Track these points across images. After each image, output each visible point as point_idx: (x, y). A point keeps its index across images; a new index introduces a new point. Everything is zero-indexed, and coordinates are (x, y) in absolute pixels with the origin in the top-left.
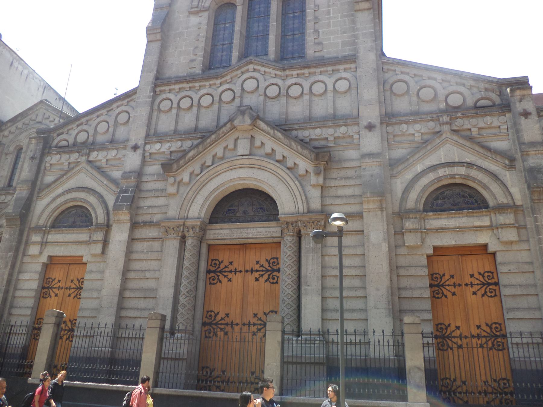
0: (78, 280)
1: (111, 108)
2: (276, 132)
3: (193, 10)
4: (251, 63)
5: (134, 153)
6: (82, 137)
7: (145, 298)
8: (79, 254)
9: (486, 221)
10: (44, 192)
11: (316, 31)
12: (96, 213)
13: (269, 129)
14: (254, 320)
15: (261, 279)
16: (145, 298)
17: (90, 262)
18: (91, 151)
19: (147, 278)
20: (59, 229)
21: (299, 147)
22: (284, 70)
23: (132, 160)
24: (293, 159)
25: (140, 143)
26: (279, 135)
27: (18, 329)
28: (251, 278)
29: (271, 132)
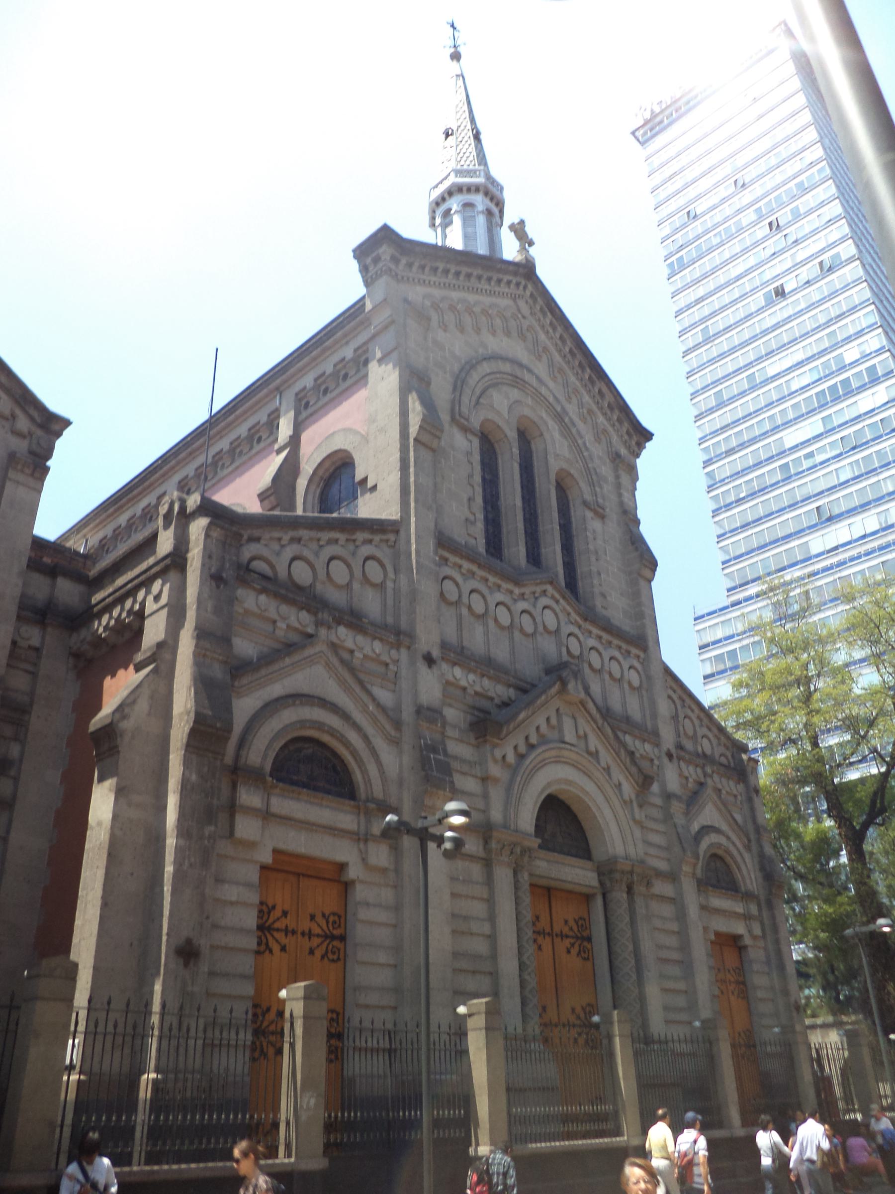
0: (324, 915)
1: (354, 537)
2: (606, 724)
3: (462, 421)
4: (551, 583)
5: (429, 671)
6: (302, 574)
7: (474, 972)
8: (340, 858)
9: (739, 908)
10: (245, 680)
11: (599, 574)
12: (365, 772)
13: (598, 716)
14: (573, 1019)
15: (572, 950)
16: (474, 972)
17: (362, 882)
18: (339, 622)
19: (472, 934)
20: (295, 788)
21: (628, 760)
22: (586, 620)
23: (429, 686)
24: (618, 775)
25: (436, 653)
26: (609, 731)
27: (369, 1040)
28: (562, 945)
29: (600, 721)
